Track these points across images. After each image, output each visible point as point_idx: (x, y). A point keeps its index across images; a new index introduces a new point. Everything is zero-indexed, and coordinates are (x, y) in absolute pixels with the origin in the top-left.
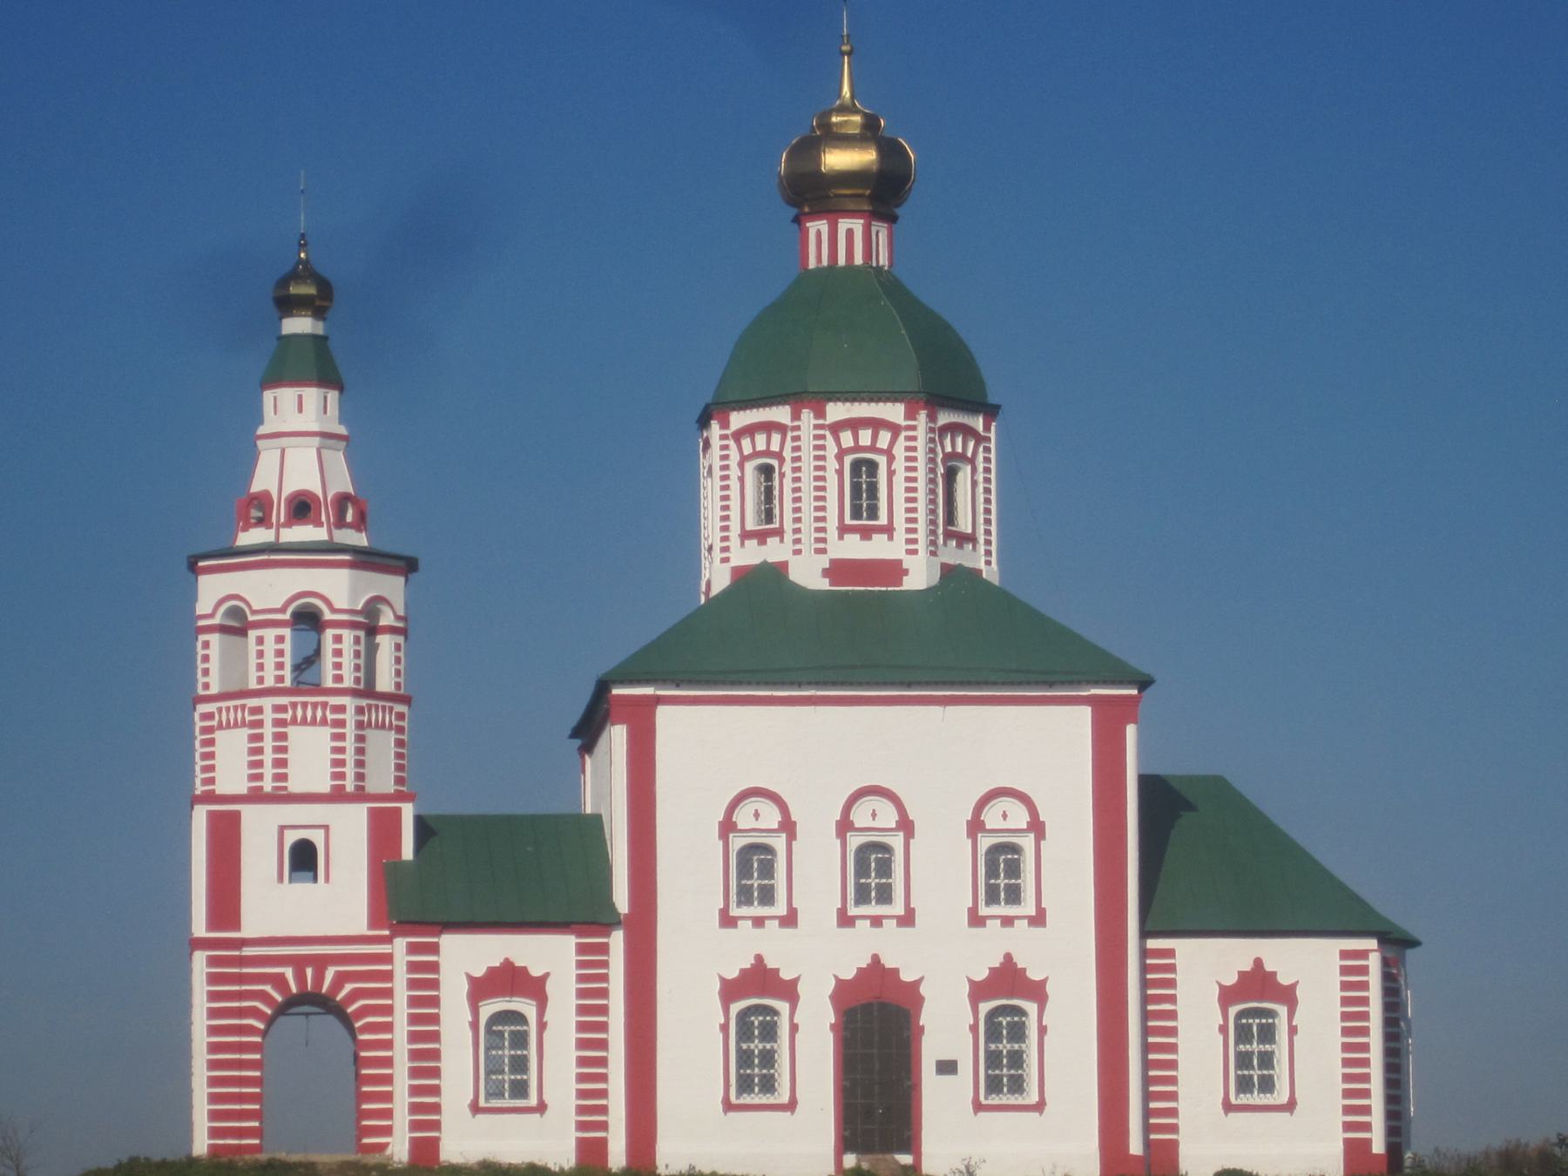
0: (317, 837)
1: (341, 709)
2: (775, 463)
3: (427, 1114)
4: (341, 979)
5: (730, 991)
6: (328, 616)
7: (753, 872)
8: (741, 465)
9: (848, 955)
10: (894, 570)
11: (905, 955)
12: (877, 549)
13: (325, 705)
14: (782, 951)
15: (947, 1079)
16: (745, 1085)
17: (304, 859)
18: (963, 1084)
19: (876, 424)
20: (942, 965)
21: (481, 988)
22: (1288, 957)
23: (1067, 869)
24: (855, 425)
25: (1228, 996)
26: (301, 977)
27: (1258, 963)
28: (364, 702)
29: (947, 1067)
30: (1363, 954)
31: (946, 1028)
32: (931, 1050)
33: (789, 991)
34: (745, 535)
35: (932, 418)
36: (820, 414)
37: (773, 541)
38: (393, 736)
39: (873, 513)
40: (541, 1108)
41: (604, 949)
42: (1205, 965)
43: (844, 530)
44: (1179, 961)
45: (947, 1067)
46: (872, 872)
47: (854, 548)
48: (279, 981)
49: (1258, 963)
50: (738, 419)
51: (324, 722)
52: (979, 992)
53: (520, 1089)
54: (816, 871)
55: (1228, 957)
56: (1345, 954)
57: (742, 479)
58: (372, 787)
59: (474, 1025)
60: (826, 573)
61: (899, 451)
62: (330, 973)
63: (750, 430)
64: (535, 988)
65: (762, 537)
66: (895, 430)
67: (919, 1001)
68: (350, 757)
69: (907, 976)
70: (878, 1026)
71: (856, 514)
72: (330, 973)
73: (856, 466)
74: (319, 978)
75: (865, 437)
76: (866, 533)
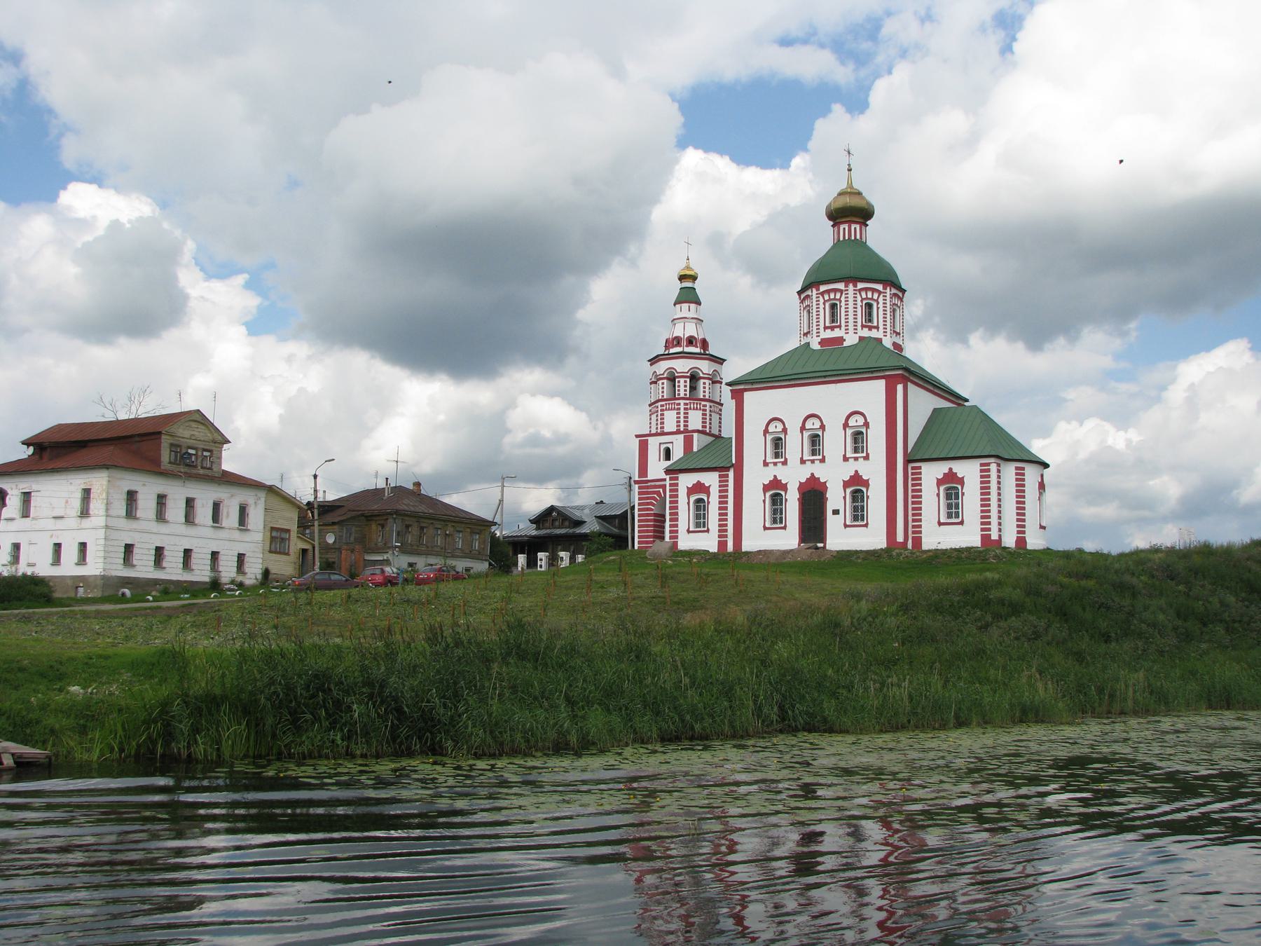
9: (803, 474)
11: (821, 472)
14: (783, 474)
20: (834, 474)
21: (691, 491)
22: (961, 468)
25: (940, 482)
27: (951, 469)
29: (836, 512)
30: (988, 464)
31: (836, 498)
32: (830, 507)
40: (708, 531)
45: (836, 512)
49: (951, 469)
52: (846, 484)
54: (795, 445)
55: (939, 469)
56: (982, 465)
69: (822, 480)
70: (813, 496)
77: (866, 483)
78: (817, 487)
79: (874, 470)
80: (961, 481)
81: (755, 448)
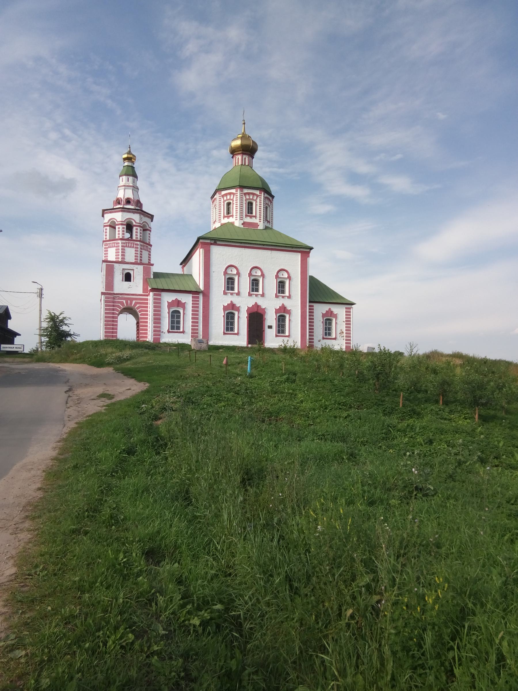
0: (131, 272)
1: (137, 245)
2: (231, 201)
3: (157, 332)
4: (136, 304)
5: (225, 308)
6: (134, 224)
7: (230, 283)
8: (224, 202)
9: (251, 302)
10: (256, 225)
11: (263, 303)
12: (253, 220)
13: (133, 244)
14: (237, 301)
15: (270, 330)
16: (227, 329)
17: (128, 277)
18: (274, 330)
19: (253, 194)
20: (270, 305)
21: (170, 305)
23: (295, 288)
24: (249, 194)
26: (127, 303)
27: (330, 309)
28: (142, 244)
29: (270, 327)
31: (271, 319)
32: (268, 323)
33: (238, 309)
34: (224, 217)
35: (264, 194)
36: (242, 191)
37: (231, 218)
38: (148, 253)
39: (252, 213)
41: (198, 297)
42: (320, 309)
43: (246, 216)
44: (314, 308)
45: (270, 327)
46: (255, 284)
47: (248, 220)
48: (122, 303)
49: (330, 309)
50: (223, 193)
51: (133, 247)
53: (178, 328)
54: (244, 284)
57: (224, 205)
58: (143, 262)
59: (169, 313)
60: (242, 224)
61: (258, 200)
62: (134, 302)
63: (226, 195)
64: (183, 305)
65: (228, 217)
66: (257, 196)
67: (265, 312)
68: (139, 255)
70: (256, 318)
71: (248, 213)
72: (134, 302)
73: (249, 203)
74: (131, 303)
75: (251, 197)
76: (251, 217)
77: (289, 312)
78: (260, 311)
79: (295, 304)
80: (336, 316)
81: (218, 283)
